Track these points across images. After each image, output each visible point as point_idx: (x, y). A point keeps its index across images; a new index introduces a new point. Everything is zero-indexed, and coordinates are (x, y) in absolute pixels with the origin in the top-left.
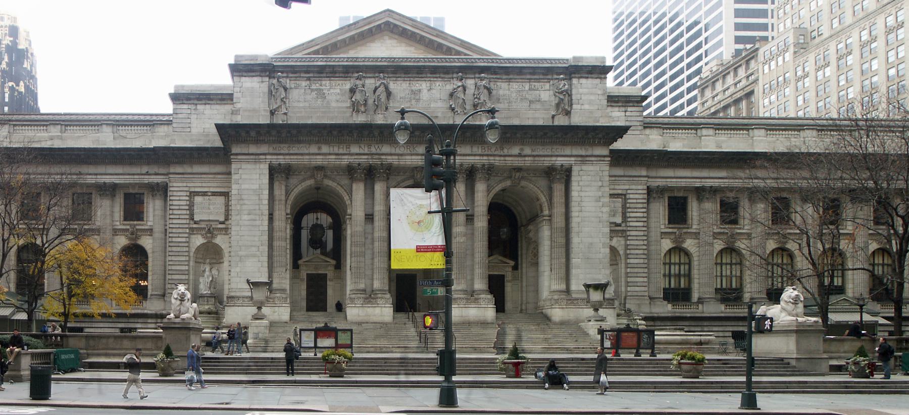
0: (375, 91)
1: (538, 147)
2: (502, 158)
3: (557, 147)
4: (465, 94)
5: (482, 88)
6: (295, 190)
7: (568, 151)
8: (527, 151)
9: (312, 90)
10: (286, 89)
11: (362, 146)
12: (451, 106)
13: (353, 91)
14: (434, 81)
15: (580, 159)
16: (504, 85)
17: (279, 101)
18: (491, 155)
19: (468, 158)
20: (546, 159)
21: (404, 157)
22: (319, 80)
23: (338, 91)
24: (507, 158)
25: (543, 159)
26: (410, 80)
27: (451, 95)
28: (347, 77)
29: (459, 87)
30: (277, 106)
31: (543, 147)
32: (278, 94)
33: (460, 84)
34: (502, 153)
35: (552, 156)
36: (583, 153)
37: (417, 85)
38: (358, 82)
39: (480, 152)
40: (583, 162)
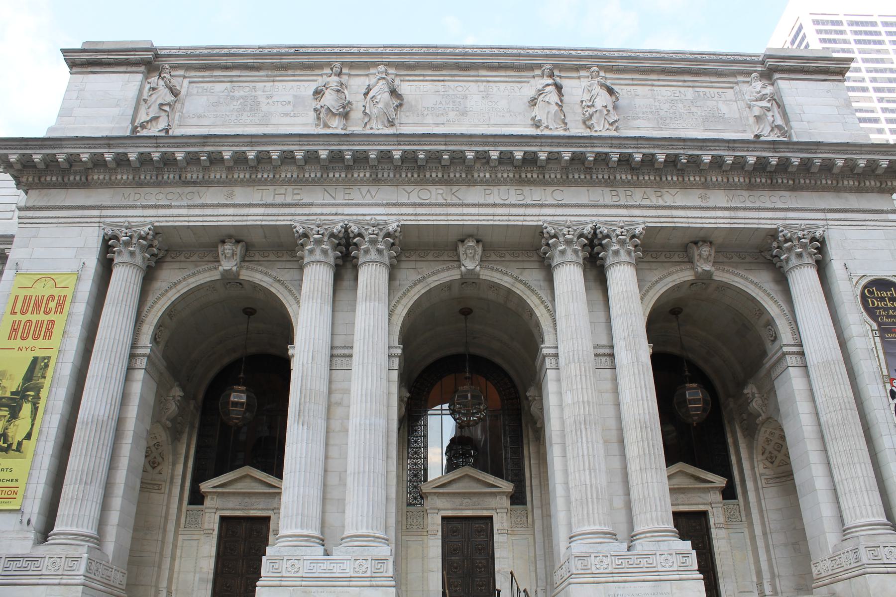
0: (366, 94)
1: (739, 192)
4: (561, 101)
5: (597, 89)
8: (719, 198)
9: (233, 98)
10: (175, 93)
12: (533, 119)
13: (318, 93)
14: (495, 82)
16: (641, 90)
17: (155, 107)
23: (291, 99)
27: (533, 102)
29: (548, 85)
30: (148, 118)
31: (751, 193)
32: (154, 97)
33: (550, 81)
34: (661, 203)
37: (460, 89)
38: (334, 81)
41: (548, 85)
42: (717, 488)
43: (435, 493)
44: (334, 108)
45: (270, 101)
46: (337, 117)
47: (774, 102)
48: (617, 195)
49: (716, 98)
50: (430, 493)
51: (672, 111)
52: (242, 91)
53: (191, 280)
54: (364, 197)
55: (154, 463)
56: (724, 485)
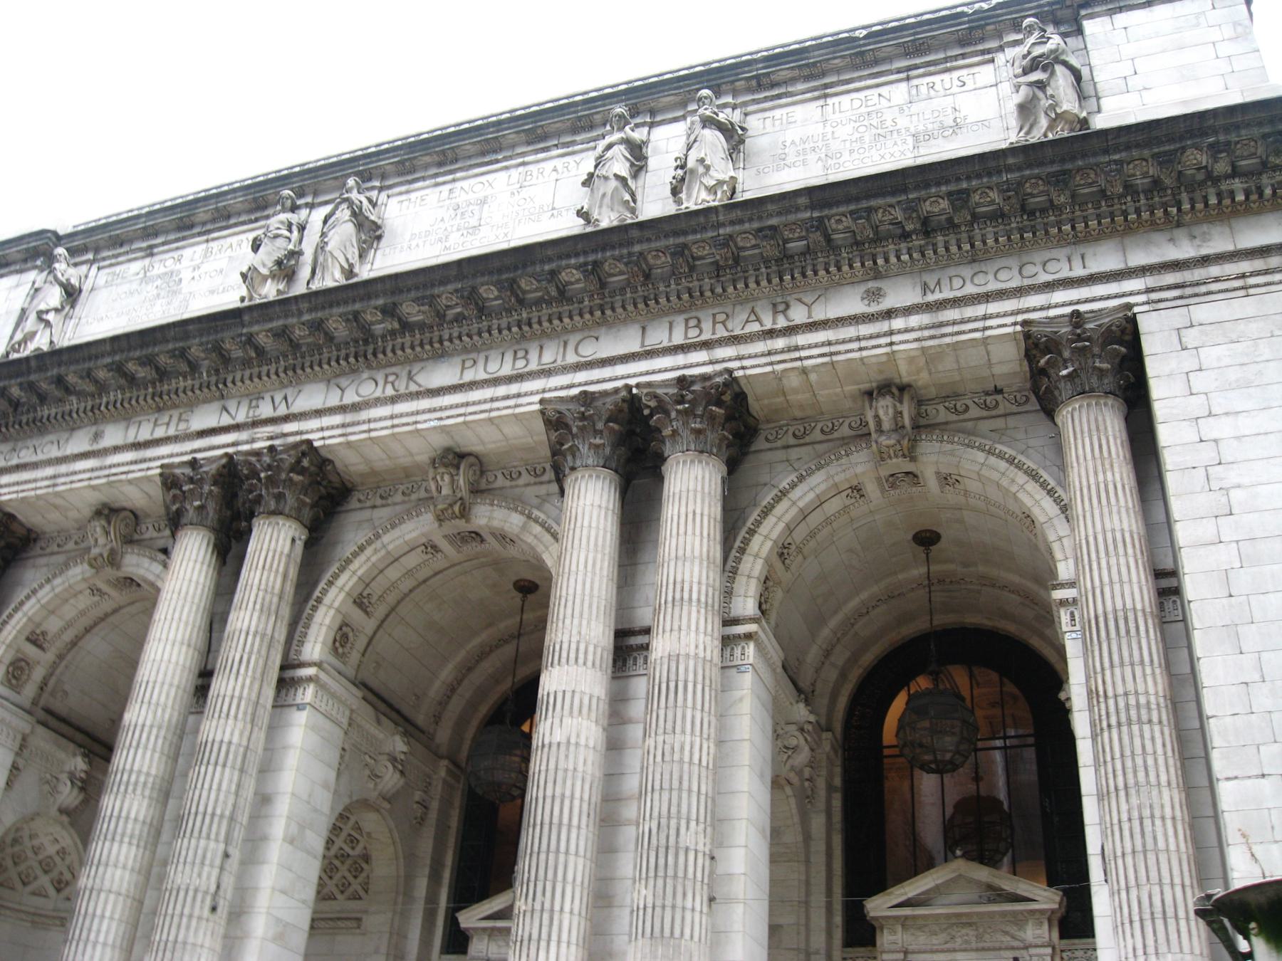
1: (952, 271)
2: (780, 343)
3: (1047, 255)
6: (26, 607)
7: (1105, 259)
11: (232, 405)
15: (1170, 278)
18: (722, 342)
19: (620, 370)
20: (993, 308)
21: (364, 415)
22: (177, 249)
24: (801, 339)
25: (980, 310)
26: (454, 180)
27: (588, 181)
28: (256, 220)
29: (610, 147)
31: (976, 267)
35: (1020, 292)
36: (1185, 250)
39: (678, 339)
40: (1188, 293)
41: (610, 147)
42: (1042, 912)
43: (484, 929)
44: (264, 265)
45: (196, 274)
46: (269, 281)
47: (1059, 69)
48: (698, 326)
49: (955, 89)
50: (476, 929)
51: (857, 135)
52: (163, 263)
53: (58, 581)
54: (275, 409)
55: (59, 882)
56: (1056, 906)
